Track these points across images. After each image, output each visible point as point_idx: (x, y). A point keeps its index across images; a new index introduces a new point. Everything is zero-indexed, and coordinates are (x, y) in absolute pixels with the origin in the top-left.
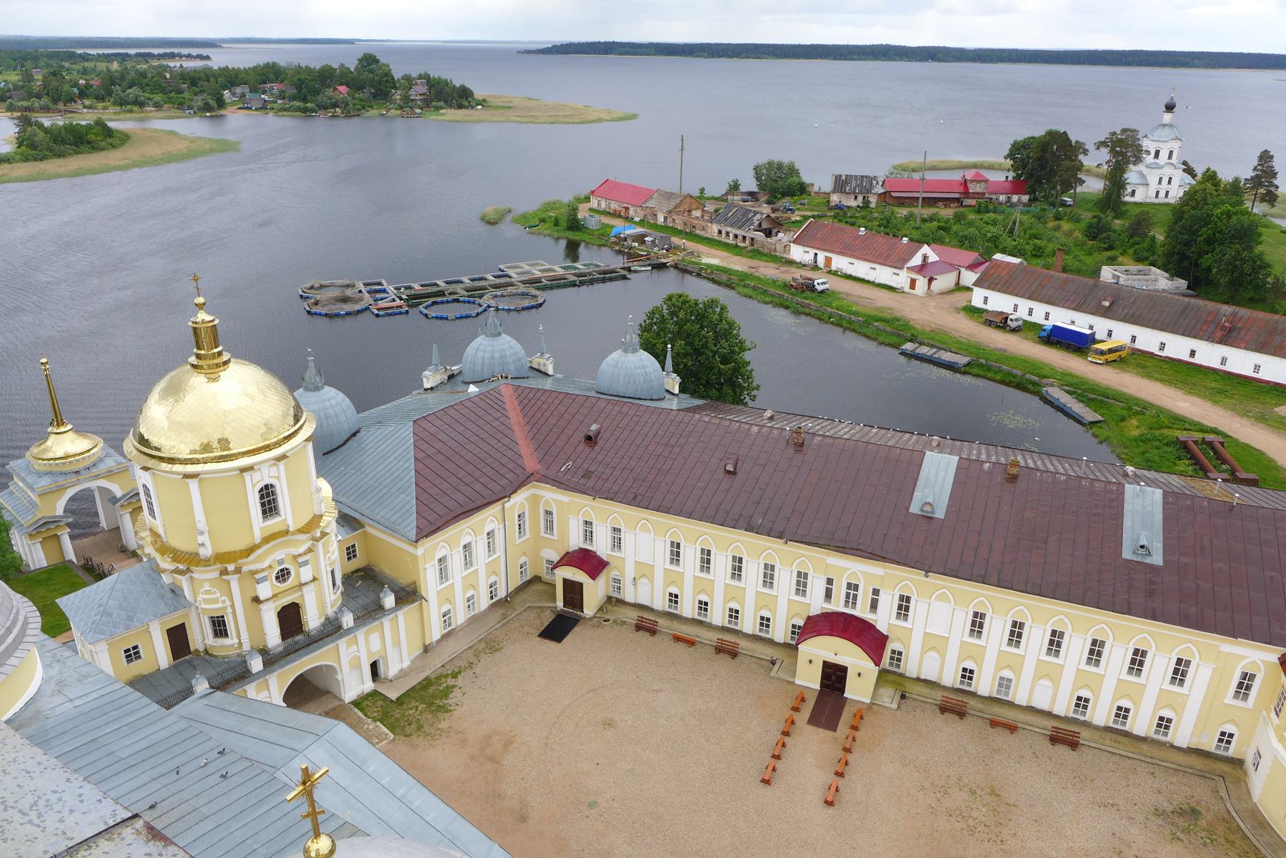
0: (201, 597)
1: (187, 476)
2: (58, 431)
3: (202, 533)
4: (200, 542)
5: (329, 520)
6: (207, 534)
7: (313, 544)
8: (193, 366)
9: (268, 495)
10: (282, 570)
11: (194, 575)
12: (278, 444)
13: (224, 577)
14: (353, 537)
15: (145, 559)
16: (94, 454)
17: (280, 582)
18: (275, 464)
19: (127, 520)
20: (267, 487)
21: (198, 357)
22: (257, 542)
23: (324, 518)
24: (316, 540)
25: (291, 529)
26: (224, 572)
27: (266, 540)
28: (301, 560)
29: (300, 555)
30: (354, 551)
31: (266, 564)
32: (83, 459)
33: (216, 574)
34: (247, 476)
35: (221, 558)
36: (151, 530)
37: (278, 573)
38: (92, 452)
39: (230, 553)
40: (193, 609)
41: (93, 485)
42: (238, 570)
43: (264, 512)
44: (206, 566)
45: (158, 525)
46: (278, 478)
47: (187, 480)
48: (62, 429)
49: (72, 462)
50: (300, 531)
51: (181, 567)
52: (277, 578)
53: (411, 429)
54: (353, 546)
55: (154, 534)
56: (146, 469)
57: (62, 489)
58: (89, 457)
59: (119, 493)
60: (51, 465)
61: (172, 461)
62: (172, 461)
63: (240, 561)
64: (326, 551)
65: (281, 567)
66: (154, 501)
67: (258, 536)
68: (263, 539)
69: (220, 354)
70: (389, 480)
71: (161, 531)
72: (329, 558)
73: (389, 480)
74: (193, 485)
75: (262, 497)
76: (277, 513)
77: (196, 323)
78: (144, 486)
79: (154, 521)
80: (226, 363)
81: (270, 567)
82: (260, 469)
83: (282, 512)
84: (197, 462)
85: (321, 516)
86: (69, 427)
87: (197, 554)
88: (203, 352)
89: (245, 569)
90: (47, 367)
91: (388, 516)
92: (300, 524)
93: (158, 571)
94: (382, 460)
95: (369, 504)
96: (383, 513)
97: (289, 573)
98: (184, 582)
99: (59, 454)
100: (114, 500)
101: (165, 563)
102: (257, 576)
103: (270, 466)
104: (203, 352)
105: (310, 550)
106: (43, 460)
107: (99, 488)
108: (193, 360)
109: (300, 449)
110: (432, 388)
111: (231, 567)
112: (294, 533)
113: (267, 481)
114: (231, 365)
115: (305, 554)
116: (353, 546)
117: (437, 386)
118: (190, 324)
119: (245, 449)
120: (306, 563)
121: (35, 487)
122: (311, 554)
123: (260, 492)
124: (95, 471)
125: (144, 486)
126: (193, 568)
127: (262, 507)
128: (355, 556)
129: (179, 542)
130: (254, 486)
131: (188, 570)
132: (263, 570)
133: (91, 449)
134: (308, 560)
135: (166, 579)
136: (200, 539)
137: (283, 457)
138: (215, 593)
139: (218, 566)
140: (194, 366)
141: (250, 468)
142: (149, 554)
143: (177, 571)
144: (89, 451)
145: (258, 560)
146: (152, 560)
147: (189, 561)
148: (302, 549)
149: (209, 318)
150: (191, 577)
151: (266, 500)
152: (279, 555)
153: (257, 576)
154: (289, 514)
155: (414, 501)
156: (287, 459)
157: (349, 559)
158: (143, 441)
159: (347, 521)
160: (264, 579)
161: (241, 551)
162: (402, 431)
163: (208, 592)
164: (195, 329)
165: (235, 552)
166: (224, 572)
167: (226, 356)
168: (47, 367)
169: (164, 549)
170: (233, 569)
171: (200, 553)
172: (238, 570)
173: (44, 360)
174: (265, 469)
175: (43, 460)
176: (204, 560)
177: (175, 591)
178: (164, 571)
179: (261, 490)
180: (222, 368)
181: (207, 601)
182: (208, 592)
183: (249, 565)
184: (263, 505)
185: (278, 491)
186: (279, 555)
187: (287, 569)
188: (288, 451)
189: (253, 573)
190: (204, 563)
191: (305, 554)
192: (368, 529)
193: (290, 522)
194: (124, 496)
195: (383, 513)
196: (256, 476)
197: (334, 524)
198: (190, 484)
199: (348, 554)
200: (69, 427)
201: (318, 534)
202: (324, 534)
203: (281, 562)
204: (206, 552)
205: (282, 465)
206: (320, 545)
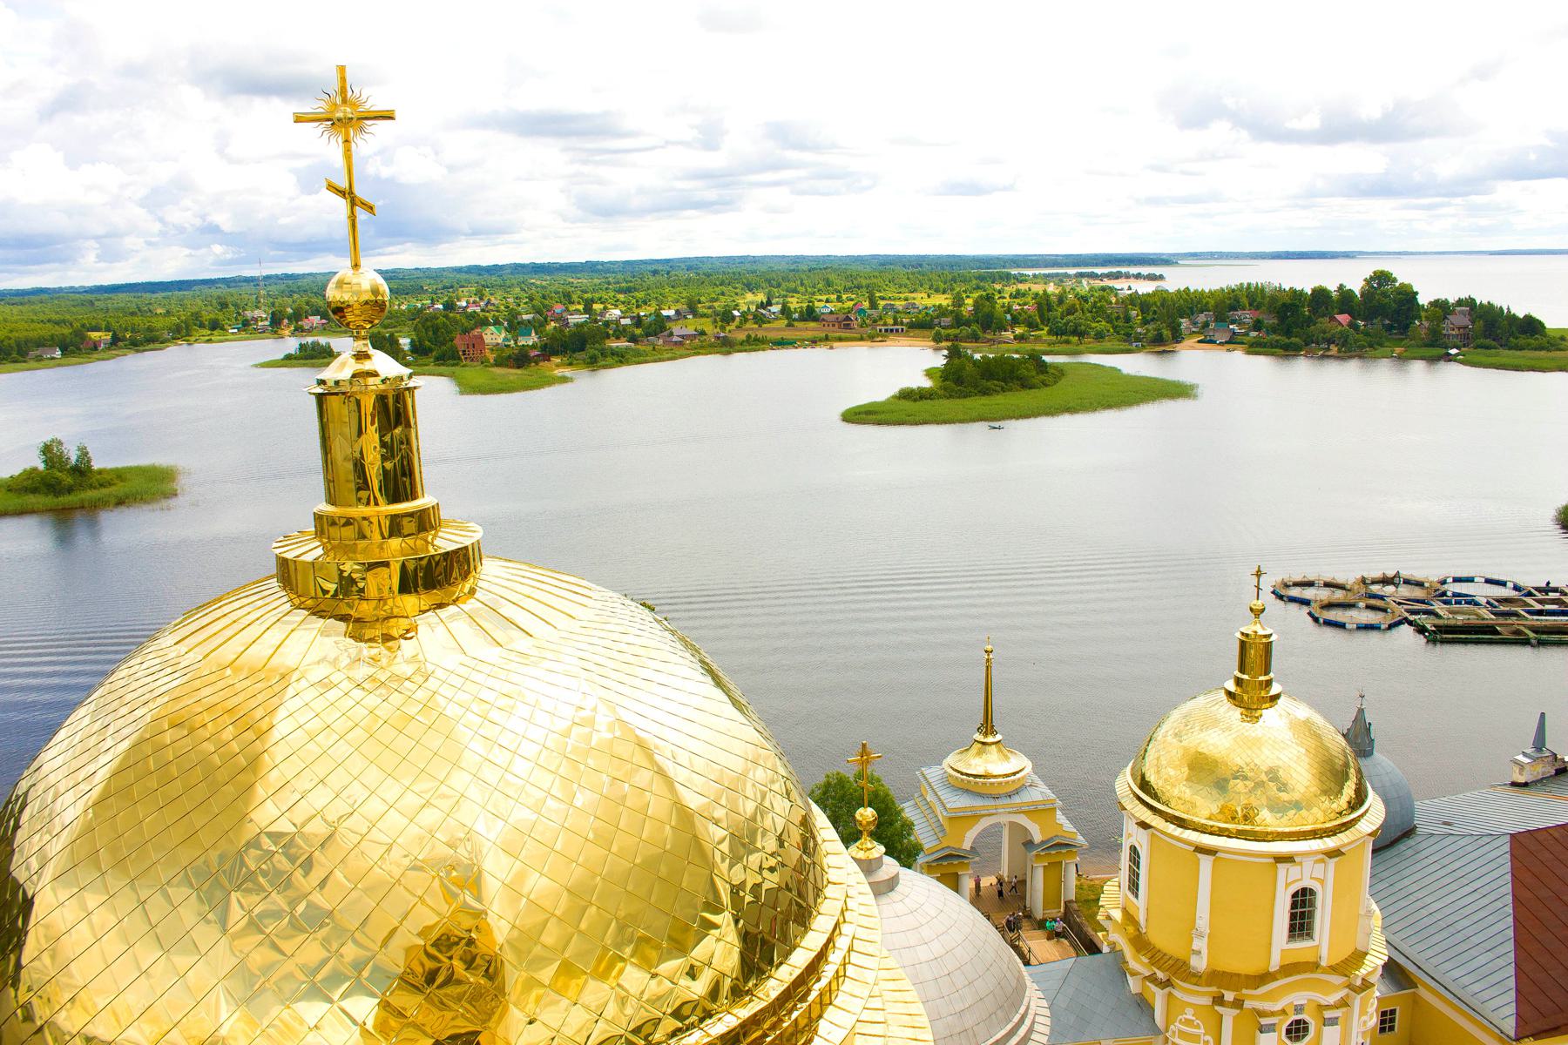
0: (1176, 1026)
1: (1201, 849)
2: (985, 740)
3: (1201, 936)
4: (1194, 947)
5: (1376, 959)
6: (1206, 938)
7: (1347, 995)
8: (1230, 694)
9: (1303, 903)
10: (1298, 1022)
11: (1175, 992)
12: (1332, 832)
13: (1217, 1008)
14: (1399, 1001)
15: (1105, 949)
16: (1019, 779)
17: (1290, 1038)
18: (1322, 861)
19: (1039, 874)
20: (1304, 891)
21: (1239, 682)
22: (1272, 970)
23: (1368, 957)
24: (1355, 992)
25: (1324, 963)
26: (1219, 1000)
27: (1289, 969)
28: (1328, 1014)
29: (1328, 1007)
30: (1392, 1020)
31: (1278, 1007)
32: (1007, 782)
33: (1207, 1001)
34: (1282, 867)
35: (1216, 978)
36: (1124, 910)
37: (1291, 1024)
38: (1018, 776)
39: (1232, 975)
40: (1161, 1037)
41: (1004, 819)
42: (1238, 1004)
43: (1292, 928)
44: (1195, 984)
45: (1140, 905)
46: (1322, 882)
47: (1200, 856)
48: (990, 739)
49: (992, 784)
50: (1333, 969)
51: (1160, 975)
52: (1288, 1031)
53: (1507, 848)
54: (1393, 1012)
55: (1129, 917)
56: (1144, 825)
57: (976, 817)
58: (1013, 781)
59: (1037, 838)
60: (969, 782)
61: (1181, 823)
62: (1181, 823)
63: (1244, 991)
64: (1363, 1012)
65: (1299, 1017)
66: (1143, 871)
67: (1275, 963)
68: (1282, 967)
69: (1269, 683)
70: (1465, 923)
71: (1141, 918)
72: (1365, 1022)
73: (1465, 923)
74: (1206, 862)
75: (1294, 905)
76: (1308, 934)
77: (1247, 635)
78: (1134, 849)
79: (1134, 900)
80: (1275, 698)
81: (1283, 1012)
82: (1301, 863)
83: (1316, 934)
84: (1220, 833)
85: (1367, 954)
86: (999, 737)
87: (1185, 964)
88: (1245, 677)
89: (1248, 1004)
90: (991, 656)
91: (1466, 980)
92: (1333, 963)
93: (1122, 971)
94: (1454, 886)
95: (1430, 953)
96: (1456, 974)
97: (1306, 1029)
98: (1158, 998)
99: (980, 771)
100: (1029, 844)
101: (1137, 963)
102: (1264, 1021)
103: (1316, 862)
104: (1245, 677)
105: (1344, 1003)
106: (962, 774)
107: (1013, 825)
108: (1231, 686)
109: (1357, 844)
110: (1526, 785)
111: (1229, 996)
112: (1325, 971)
113: (1307, 883)
114: (1283, 698)
115: (1336, 1006)
116: (1393, 1012)
117: (1535, 782)
118: (1238, 635)
119: (1287, 830)
120: (1333, 1022)
121: (948, 806)
122: (1344, 1009)
123: (1293, 896)
124: (1017, 800)
125: (1134, 849)
126: (1176, 981)
127: (1291, 920)
128: (1392, 1028)
129: (1161, 939)
130: (1287, 885)
131: (1167, 984)
132: (1272, 1014)
133: (1017, 772)
134: (1337, 1018)
135: (1134, 985)
136: (1197, 944)
137: (1335, 853)
138: (1198, 1026)
139: (1214, 989)
140: (1230, 694)
141: (1288, 859)
142: (1114, 943)
143: (1152, 979)
144: (1014, 774)
145: (1270, 996)
146: (1116, 953)
147: (1175, 971)
148: (1333, 999)
149: (1268, 632)
150: (1170, 994)
151: (1299, 910)
152: (1300, 997)
153: (1264, 1021)
154: (1324, 941)
155: (1511, 970)
156: (1344, 856)
157: (1382, 1030)
158: (1145, 785)
159: (1394, 971)
160: (1271, 1028)
161: (1248, 977)
162: (1487, 848)
163: (1188, 1022)
164: (1243, 644)
165: (1239, 975)
166: (1219, 1000)
167: (1276, 689)
168: (991, 656)
169: (1140, 943)
170: (1232, 1000)
171: (1191, 963)
172: (1238, 1004)
173: (989, 648)
174: (1308, 864)
175: (962, 774)
176: (1194, 975)
177: (1143, 1005)
178: (1134, 974)
179: (1295, 895)
180: (1268, 705)
181: (1183, 1035)
182: (1188, 1022)
183: (1255, 1000)
184: (1293, 917)
185: (1318, 903)
186: (1300, 997)
187: (1305, 1022)
188: (1344, 845)
189: (1262, 1014)
190: (1194, 980)
191: (1336, 1006)
192: (1422, 991)
193: (1324, 952)
194: (1043, 842)
195: (1456, 974)
196: (1294, 871)
197: (1380, 971)
198: (1201, 861)
199: (1382, 1022)
200: (999, 737)
201: (1359, 982)
202: (1366, 985)
203: (1299, 1009)
204: (1200, 964)
205: (1332, 862)
206: (1357, 1001)
